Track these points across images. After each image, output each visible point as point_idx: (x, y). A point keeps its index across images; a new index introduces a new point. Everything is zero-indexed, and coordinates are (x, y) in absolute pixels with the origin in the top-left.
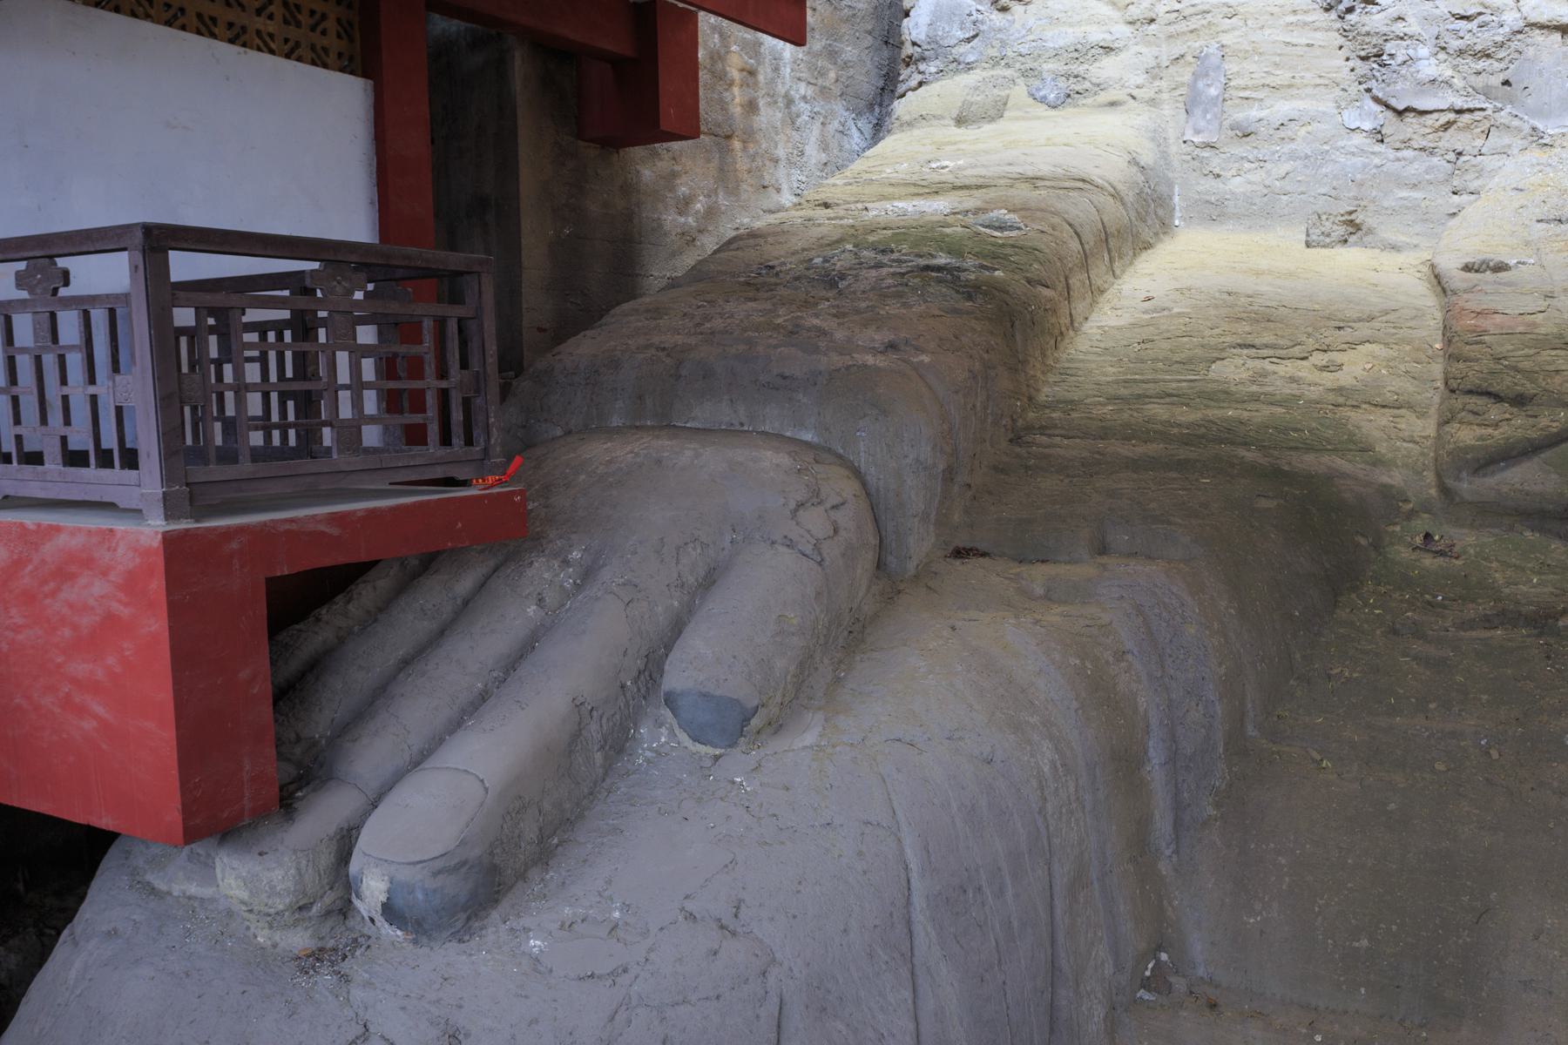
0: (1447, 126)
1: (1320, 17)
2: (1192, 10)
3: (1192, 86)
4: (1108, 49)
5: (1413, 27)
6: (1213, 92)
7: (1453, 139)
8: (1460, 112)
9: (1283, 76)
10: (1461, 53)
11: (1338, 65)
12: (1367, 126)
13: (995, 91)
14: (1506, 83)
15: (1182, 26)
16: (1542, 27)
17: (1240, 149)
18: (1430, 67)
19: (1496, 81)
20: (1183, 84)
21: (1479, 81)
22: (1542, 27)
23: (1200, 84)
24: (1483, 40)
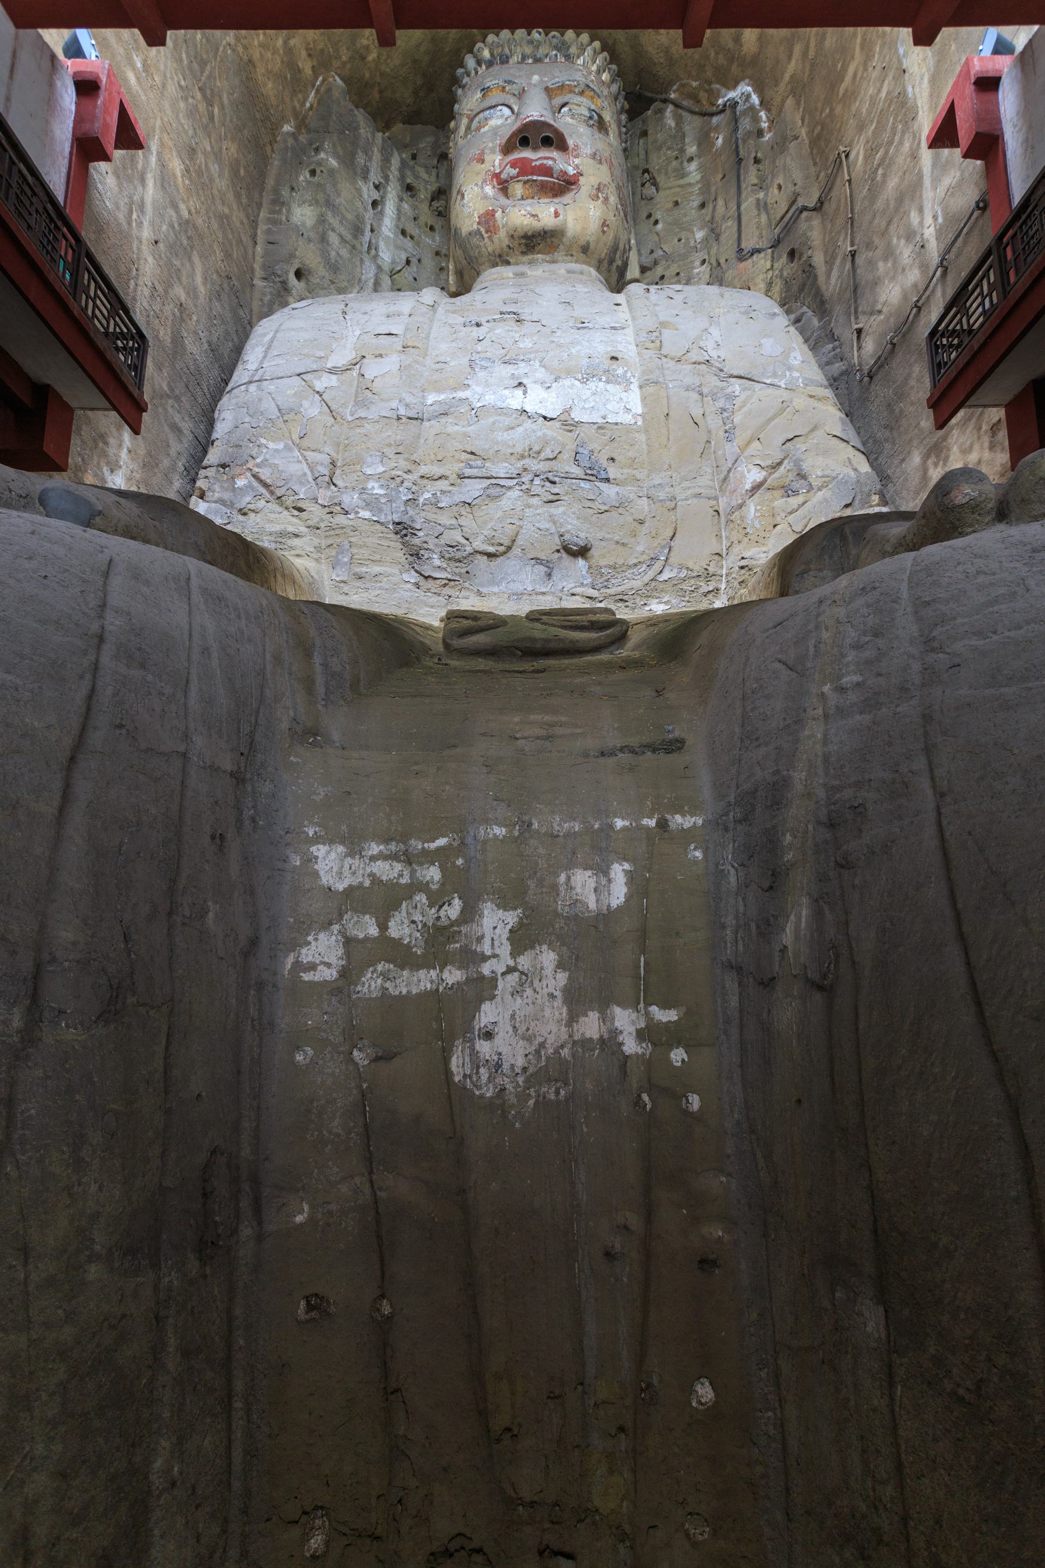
0: (445, 585)
1: (393, 536)
3: (336, 557)
4: (296, 536)
5: (431, 547)
6: (346, 560)
7: (447, 591)
8: (450, 580)
9: (377, 557)
10: (450, 559)
11: (400, 555)
12: (412, 581)
14: (467, 572)
15: (332, 533)
16: (480, 553)
17: (358, 584)
18: (437, 562)
19: (464, 571)
21: (457, 570)
22: (480, 553)
23: (340, 557)
24: (458, 555)
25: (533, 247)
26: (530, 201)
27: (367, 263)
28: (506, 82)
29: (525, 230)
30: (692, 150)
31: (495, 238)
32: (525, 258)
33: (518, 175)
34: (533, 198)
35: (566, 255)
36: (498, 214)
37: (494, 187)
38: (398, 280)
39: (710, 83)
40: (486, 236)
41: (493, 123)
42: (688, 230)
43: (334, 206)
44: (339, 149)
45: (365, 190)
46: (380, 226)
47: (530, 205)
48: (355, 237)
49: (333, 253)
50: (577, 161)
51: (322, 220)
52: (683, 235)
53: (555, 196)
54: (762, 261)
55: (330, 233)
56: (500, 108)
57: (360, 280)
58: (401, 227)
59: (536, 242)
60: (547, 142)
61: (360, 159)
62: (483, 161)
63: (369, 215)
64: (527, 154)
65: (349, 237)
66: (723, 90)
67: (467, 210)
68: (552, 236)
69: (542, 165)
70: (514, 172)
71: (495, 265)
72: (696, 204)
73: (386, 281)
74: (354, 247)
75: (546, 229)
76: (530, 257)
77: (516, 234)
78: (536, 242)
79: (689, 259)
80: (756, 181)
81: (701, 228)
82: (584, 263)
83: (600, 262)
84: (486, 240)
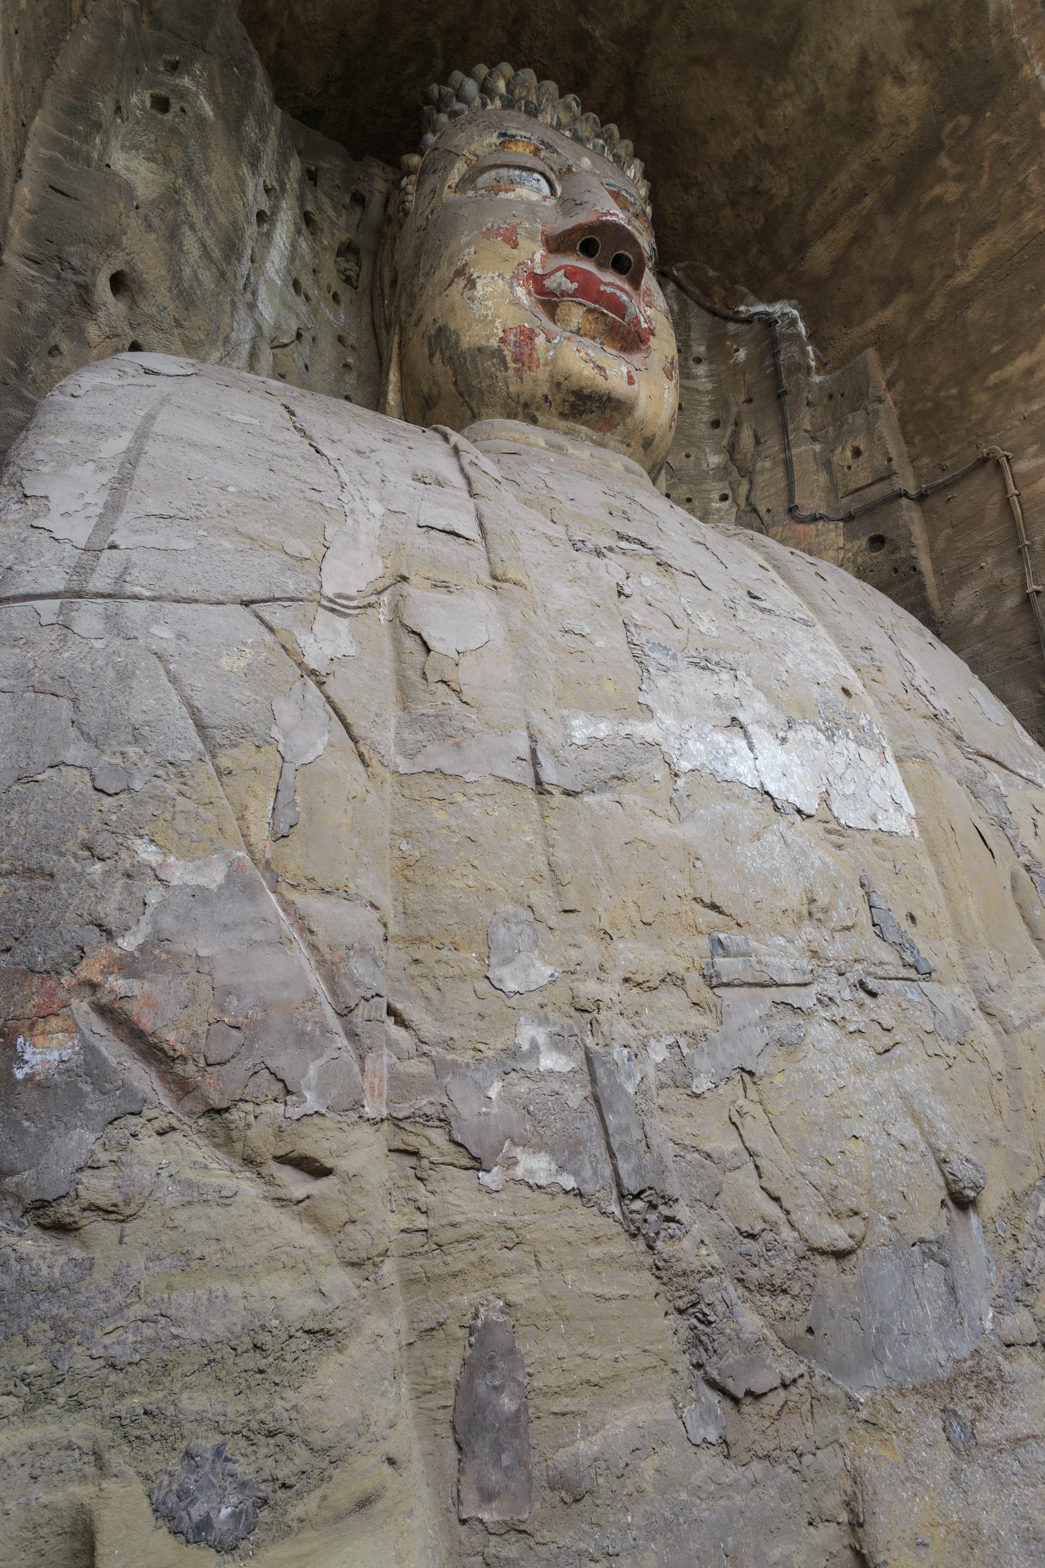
2: (451, 1234)
3: (464, 1389)
13: (41, 1494)
16: (823, 1253)
20: (445, 1383)
22: (823, 1253)
23: (481, 1387)
25: (581, 413)
26: (587, 341)
28: (543, 142)
29: (583, 384)
30: (700, 350)
31: (528, 376)
32: (562, 424)
34: (593, 338)
35: (622, 442)
36: (540, 340)
37: (529, 293)
39: (734, 282)
40: (512, 365)
41: (523, 192)
42: (699, 448)
47: (594, 349)
50: (649, 312)
52: (693, 451)
54: (833, 535)
56: (536, 176)
58: (294, 274)
59: (590, 408)
60: (620, 265)
62: (515, 246)
64: (587, 266)
66: (751, 298)
67: (478, 310)
69: (613, 294)
70: (571, 286)
71: (511, 415)
72: (707, 417)
73: (266, 356)
75: (613, 395)
76: (571, 424)
78: (590, 408)
79: (704, 487)
80: (809, 428)
81: (717, 452)
82: (638, 461)
83: (654, 466)
84: (511, 372)
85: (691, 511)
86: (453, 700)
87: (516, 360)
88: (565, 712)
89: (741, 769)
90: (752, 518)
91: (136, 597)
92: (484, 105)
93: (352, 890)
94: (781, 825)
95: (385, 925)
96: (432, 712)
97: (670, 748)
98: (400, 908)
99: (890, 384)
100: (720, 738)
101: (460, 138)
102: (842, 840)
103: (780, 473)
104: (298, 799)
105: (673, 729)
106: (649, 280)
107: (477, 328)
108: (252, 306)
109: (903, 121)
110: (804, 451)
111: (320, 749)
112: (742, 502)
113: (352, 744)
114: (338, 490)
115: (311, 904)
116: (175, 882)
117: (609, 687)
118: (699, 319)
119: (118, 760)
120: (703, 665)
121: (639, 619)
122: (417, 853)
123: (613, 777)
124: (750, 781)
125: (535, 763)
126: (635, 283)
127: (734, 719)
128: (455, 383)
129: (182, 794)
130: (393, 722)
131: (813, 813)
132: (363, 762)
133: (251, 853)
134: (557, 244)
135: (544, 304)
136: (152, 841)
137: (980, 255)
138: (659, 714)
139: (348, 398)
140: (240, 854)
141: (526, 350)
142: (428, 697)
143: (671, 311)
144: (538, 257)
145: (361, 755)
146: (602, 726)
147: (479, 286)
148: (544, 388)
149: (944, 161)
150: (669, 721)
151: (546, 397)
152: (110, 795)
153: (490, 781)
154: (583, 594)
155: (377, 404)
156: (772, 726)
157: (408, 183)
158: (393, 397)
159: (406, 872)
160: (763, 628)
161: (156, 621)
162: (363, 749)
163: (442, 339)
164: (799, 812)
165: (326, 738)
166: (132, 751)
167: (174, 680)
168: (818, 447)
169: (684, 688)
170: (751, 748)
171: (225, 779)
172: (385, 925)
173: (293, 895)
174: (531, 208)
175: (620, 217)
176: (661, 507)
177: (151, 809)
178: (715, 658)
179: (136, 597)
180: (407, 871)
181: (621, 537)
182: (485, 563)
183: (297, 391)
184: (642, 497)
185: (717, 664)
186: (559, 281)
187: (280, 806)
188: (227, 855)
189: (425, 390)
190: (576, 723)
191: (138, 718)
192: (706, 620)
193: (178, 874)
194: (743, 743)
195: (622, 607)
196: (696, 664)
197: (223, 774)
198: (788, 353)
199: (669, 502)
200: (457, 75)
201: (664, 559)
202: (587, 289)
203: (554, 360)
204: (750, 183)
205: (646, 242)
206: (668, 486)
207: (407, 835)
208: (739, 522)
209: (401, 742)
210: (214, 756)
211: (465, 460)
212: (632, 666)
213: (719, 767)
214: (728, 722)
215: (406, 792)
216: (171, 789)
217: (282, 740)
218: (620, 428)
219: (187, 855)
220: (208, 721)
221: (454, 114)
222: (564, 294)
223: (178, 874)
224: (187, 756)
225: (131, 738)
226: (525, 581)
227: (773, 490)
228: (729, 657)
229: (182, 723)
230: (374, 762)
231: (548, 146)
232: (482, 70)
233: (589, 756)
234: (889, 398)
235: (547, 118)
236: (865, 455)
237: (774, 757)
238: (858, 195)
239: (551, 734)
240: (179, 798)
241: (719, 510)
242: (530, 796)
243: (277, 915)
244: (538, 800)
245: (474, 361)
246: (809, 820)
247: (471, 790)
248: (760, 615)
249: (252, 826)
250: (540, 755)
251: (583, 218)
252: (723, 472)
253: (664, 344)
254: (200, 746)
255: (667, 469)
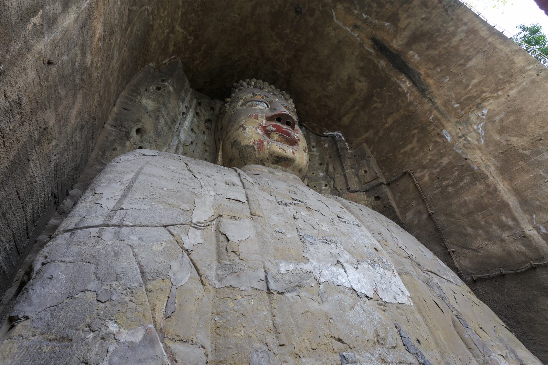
27: (175, 137)
30: (314, 144)
31: (262, 153)
32: (273, 166)
33: (275, 131)
36: (265, 143)
38: (187, 150)
41: (260, 107)
43: (166, 107)
44: (175, 85)
45: (181, 106)
46: (183, 123)
48: (172, 124)
49: (160, 127)
51: (158, 110)
52: (315, 172)
53: (290, 145)
55: (161, 117)
57: (169, 145)
59: (281, 161)
60: (288, 124)
61: (183, 94)
62: (257, 119)
63: (180, 117)
64: (279, 124)
65: (169, 123)
68: (289, 161)
71: (257, 163)
73: (181, 149)
74: (170, 128)
76: (276, 166)
77: (273, 155)
78: (281, 161)
81: (322, 172)
84: (256, 152)
85: (316, 190)
86: (237, 258)
87: (258, 149)
88: (277, 261)
89: (343, 281)
90: (336, 192)
91: (127, 226)
92: (248, 87)
93: (194, 340)
94: (361, 303)
95: (207, 356)
96: (229, 263)
97: (316, 272)
98: (214, 347)
99: (372, 153)
100: (334, 268)
101: (242, 95)
102: (385, 308)
103: (343, 178)
104: (176, 300)
105: (317, 266)
106: (297, 127)
107: (246, 140)
108: (178, 136)
109: (362, 90)
110: (349, 172)
111: (186, 279)
112: (332, 187)
113: (199, 277)
114: (200, 188)
115: (178, 348)
116: (122, 340)
117: (293, 251)
118: (312, 136)
119: (108, 288)
120: (325, 242)
121: (301, 227)
122: (221, 322)
123: (296, 286)
124: (347, 285)
125: (267, 281)
126: (293, 128)
127: (338, 261)
128: (239, 155)
129: (131, 301)
130: (215, 267)
131: (372, 297)
132: (203, 284)
133: (155, 325)
134: (269, 119)
135: (266, 133)
136: (116, 322)
137: (390, 120)
138: (311, 260)
139: (206, 160)
140: (151, 326)
141: (261, 146)
142: (228, 258)
143: (304, 134)
144: (264, 122)
145: (202, 281)
146: (291, 266)
147: (247, 129)
148: (267, 156)
149: (375, 99)
150: (315, 263)
151: (268, 158)
152: (102, 303)
153: (250, 290)
154: (282, 219)
155: (214, 161)
156: (352, 263)
157: (227, 105)
158: (220, 159)
159: (217, 330)
160: (344, 228)
161: (132, 234)
162: (203, 279)
163: (235, 143)
164: (367, 297)
165: (189, 275)
166: (115, 284)
167: (135, 255)
168: (353, 170)
169: (319, 250)
170: (346, 272)
171: (149, 294)
172: (207, 356)
173: (170, 344)
174: (262, 111)
175: (287, 112)
176: (306, 189)
177: (118, 308)
178: (329, 239)
179: (127, 226)
180: (218, 330)
181: (294, 200)
182: (249, 210)
183: (189, 159)
184: (300, 187)
185: (330, 241)
186: (270, 128)
187: (169, 304)
188: (145, 327)
189: (230, 157)
190: (281, 265)
191: (118, 270)
192: (324, 226)
193: (124, 336)
194: (343, 270)
195: (295, 223)
196: (323, 242)
197: (148, 291)
198: (340, 145)
199: (308, 188)
200: (241, 81)
201: (308, 206)
202: (279, 130)
203: (270, 148)
204: (323, 104)
205: (295, 118)
206: (308, 183)
207: (218, 314)
208: (332, 193)
209: (217, 275)
210: (146, 284)
211: (242, 177)
212: (300, 243)
213: (335, 280)
214: (336, 262)
215: (218, 295)
216: (127, 299)
217: (172, 277)
218: (291, 166)
219: (129, 327)
220: (145, 271)
221: (240, 90)
222: (272, 131)
223: (124, 336)
224: (135, 285)
225: (115, 278)
226: (262, 215)
227: (341, 183)
228: (334, 239)
229: (136, 272)
230: (207, 284)
231: (266, 96)
232: (248, 80)
233: (287, 278)
234: (372, 156)
235: (266, 90)
236: (368, 172)
237: (354, 275)
238: (353, 106)
239: (273, 270)
240: (130, 303)
241: (325, 189)
242: (265, 295)
243: (162, 354)
244: (268, 297)
245: (245, 149)
246: (371, 300)
247: (243, 294)
248: (342, 224)
249: (157, 313)
250: (269, 278)
251: (277, 113)
252: (325, 178)
253: (303, 143)
254: (141, 281)
255: (307, 178)
